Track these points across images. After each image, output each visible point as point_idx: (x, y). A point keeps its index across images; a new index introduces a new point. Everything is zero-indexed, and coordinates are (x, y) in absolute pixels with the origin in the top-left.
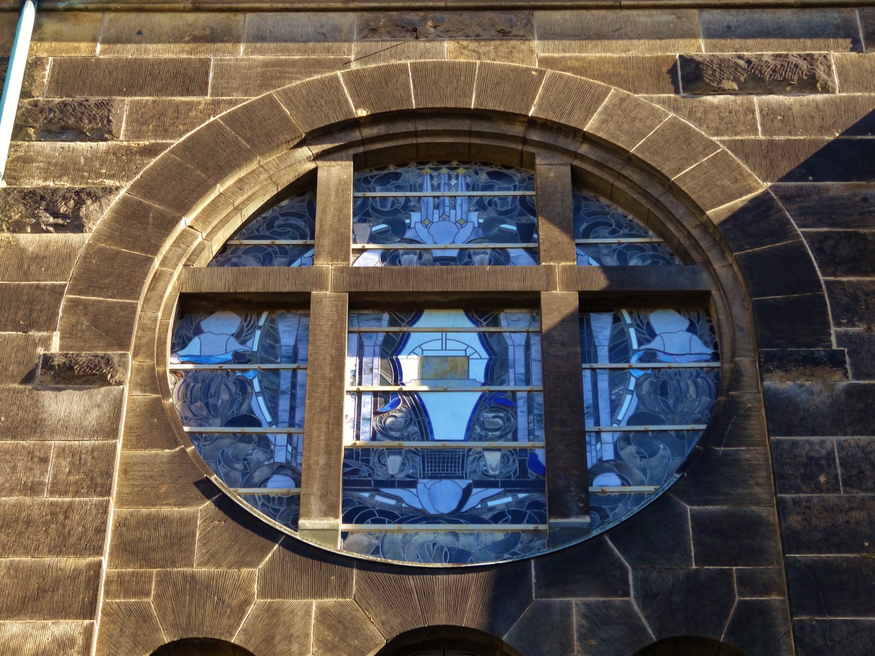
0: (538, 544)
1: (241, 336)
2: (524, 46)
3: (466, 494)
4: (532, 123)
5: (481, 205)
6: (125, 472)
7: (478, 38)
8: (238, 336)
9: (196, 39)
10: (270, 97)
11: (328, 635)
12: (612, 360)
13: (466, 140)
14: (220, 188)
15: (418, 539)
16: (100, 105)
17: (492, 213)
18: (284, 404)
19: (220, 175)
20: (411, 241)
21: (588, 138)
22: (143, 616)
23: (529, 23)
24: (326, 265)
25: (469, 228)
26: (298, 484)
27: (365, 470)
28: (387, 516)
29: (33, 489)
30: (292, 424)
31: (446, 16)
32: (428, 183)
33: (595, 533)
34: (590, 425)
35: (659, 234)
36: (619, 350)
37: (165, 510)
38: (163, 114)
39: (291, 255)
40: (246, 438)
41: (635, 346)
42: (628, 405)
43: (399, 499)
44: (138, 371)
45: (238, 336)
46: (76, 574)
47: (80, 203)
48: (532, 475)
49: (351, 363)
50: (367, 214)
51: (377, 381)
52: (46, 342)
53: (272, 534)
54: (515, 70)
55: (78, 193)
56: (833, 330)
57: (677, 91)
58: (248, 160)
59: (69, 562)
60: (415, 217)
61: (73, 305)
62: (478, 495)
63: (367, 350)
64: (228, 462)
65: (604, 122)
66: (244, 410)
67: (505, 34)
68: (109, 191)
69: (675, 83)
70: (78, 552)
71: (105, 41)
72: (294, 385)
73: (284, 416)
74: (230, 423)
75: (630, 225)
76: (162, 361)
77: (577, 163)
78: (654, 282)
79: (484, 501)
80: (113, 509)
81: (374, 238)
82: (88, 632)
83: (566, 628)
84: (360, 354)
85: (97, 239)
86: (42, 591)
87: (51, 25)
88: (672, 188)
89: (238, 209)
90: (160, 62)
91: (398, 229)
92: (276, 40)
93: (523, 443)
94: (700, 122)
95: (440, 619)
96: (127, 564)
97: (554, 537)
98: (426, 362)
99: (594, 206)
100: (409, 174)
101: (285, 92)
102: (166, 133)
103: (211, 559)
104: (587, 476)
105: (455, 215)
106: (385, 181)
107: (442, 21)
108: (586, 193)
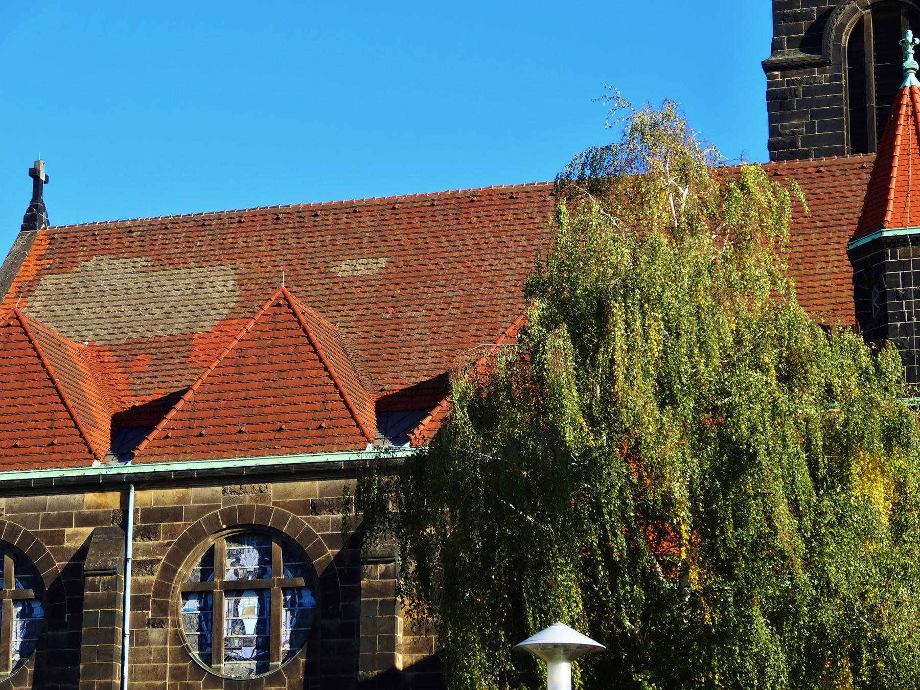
19: (187, 554)
20: (242, 565)
24: (217, 580)
27: (229, 645)
28: (235, 659)
29: (149, 661)
59: (159, 683)
60: (243, 555)
65: (288, 527)
68: (159, 561)
73: (210, 628)
91: (238, 560)
94: (314, 527)
102: (172, 537)
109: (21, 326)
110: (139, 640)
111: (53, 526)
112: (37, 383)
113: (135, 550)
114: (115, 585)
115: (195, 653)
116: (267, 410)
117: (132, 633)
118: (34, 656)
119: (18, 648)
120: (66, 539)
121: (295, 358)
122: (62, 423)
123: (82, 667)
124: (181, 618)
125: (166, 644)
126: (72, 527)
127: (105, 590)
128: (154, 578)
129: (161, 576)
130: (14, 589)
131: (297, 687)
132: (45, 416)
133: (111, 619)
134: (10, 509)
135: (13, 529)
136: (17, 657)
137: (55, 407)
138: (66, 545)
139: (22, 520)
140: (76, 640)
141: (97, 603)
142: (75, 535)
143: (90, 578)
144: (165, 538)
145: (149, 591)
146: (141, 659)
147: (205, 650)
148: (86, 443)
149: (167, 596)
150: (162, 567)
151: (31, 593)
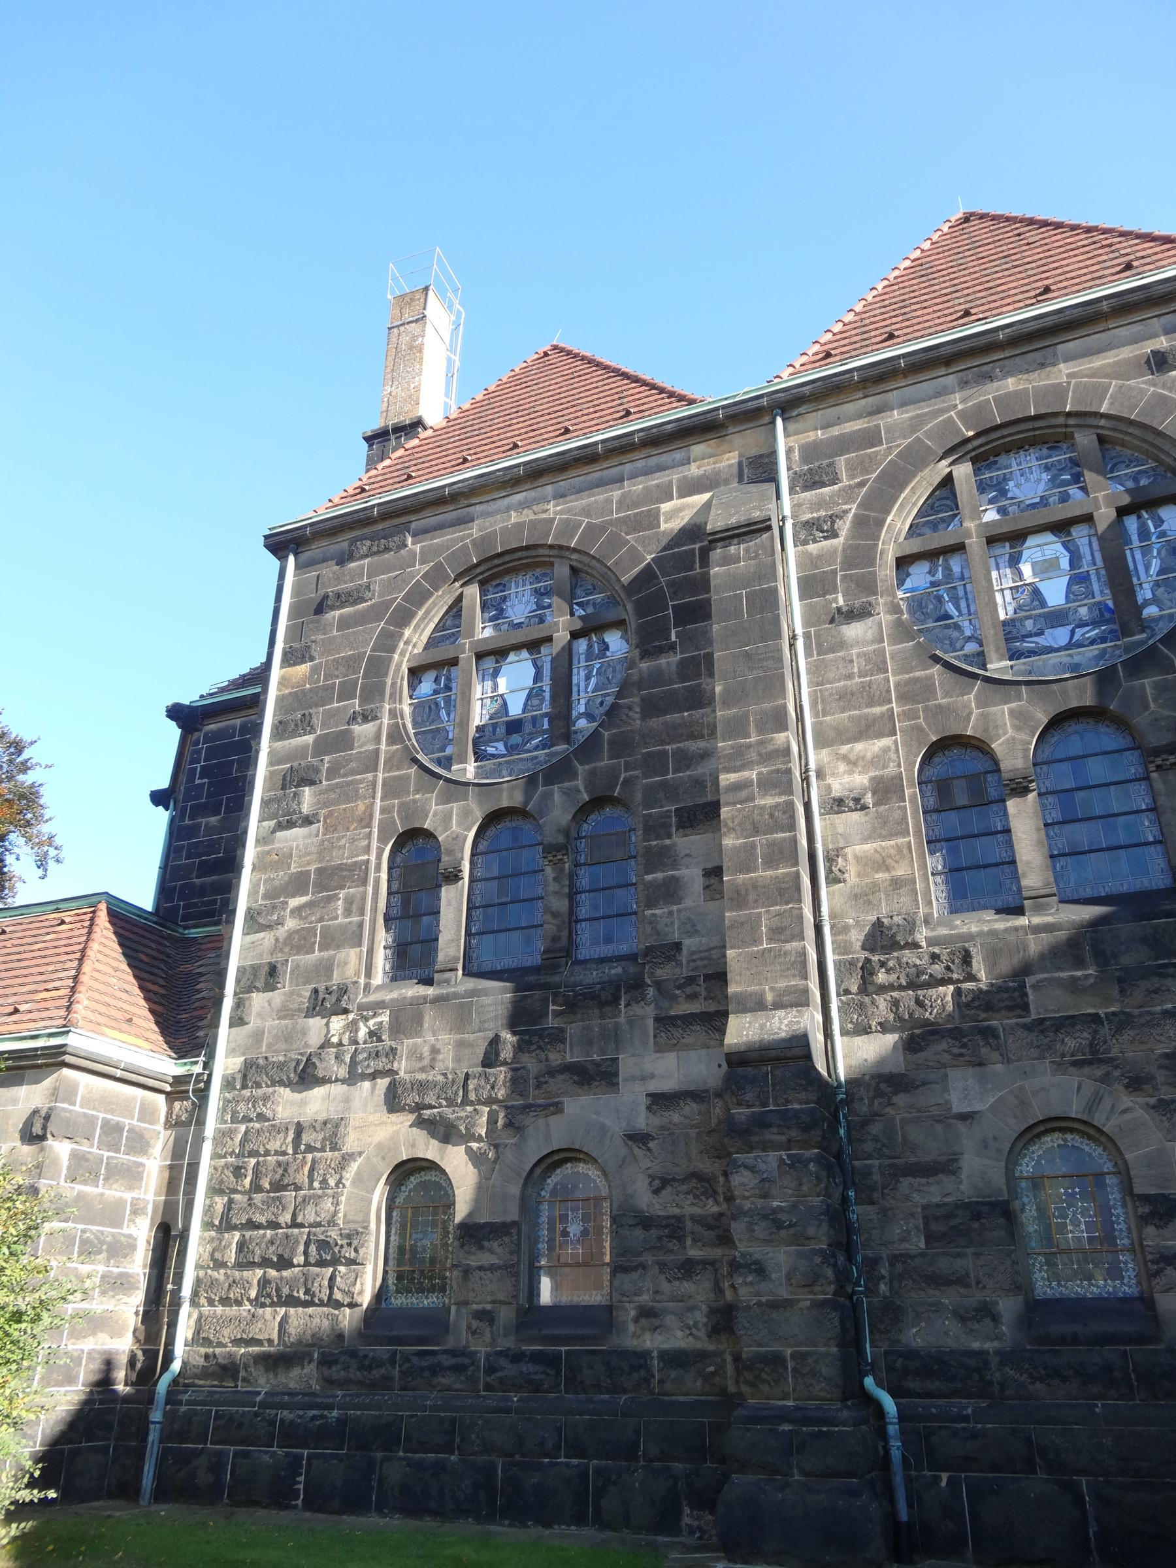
0: (1117, 652)
1: (931, 572)
2: (1055, 369)
3: (1073, 633)
4: (1069, 415)
5: (1047, 468)
6: (892, 658)
7: (1027, 372)
8: (929, 572)
9: (871, 414)
10: (918, 439)
11: (1017, 722)
12: (1141, 541)
13: (1032, 433)
14: (903, 496)
15: (1052, 662)
16: (829, 465)
17: (1054, 471)
18: (963, 604)
19: (902, 488)
21: (1103, 416)
22: (920, 729)
23: (1055, 354)
24: (970, 525)
25: (1043, 482)
26: (981, 645)
28: (1032, 653)
29: (850, 677)
30: (970, 614)
31: (1006, 362)
32: (1014, 463)
33: (1151, 642)
34: (1135, 581)
35: (1156, 461)
36: (1144, 534)
37: (917, 674)
38: (862, 462)
39: (947, 521)
40: (947, 627)
41: (1153, 530)
42: (1155, 565)
43: (1037, 643)
44: (885, 604)
45: (929, 572)
46: (882, 715)
47: (833, 522)
48: (1107, 615)
49: (994, 574)
50: (984, 489)
51: (1010, 581)
52: (836, 600)
53: (975, 676)
54: (1053, 385)
55: (831, 517)
57: (1153, 374)
58: (914, 476)
59: (877, 710)
60: (1011, 484)
61: (844, 578)
62: (1079, 632)
63: (1001, 565)
64: (942, 642)
65: (1112, 404)
66: (942, 612)
67: (1042, 365)
68: (846, 512)
69: (1150, 368)
70: (881, 704)
71: (823, 428)
72: (966, 593)
73: (964, 611)
74: (938, 620)
75: (1137, 460)
76: (895, 596)
77: (1099, 431)
78: (1159, 492)
79: (1083, 635)
81: (991, 502)
82: (896, 742)
83: (1143, 697)
84: (998, 569)
85: (846, 539)
86: (868, 727)
87: (792, 427)
88: (1159, 434)
89: (914, 504)
90: (854, 432)
91: (1003, 493)
92: (914, 403)
93: (1098, 598)
95: (1074, 704)
96: (905, 705)
97: (1127, 649)
98: (1034, 565)
99: (1113, 453)
100: (1002, 460)
101: (925, 432)
102: (868, 472)
103: (947, 694)
104: (1139, 609)
105: (1034, 477)
106: (989, 467)
107: (1004, 366)
108: (1108, 446)
110: (820, 646)
111: (636, 504)
113: (796, 507)
117: (807, 636)
120: (662, 518)
123: (718, 689)
126: (671, 499)
127: (751, 558)
135: (568, 525)
138: (664, 526)
139: (583, 509)
141: (737, 582)
144: (852, 477)
145: (834, 562)
146: (831, 675)
147: (962, 648)
150: (853, 522)
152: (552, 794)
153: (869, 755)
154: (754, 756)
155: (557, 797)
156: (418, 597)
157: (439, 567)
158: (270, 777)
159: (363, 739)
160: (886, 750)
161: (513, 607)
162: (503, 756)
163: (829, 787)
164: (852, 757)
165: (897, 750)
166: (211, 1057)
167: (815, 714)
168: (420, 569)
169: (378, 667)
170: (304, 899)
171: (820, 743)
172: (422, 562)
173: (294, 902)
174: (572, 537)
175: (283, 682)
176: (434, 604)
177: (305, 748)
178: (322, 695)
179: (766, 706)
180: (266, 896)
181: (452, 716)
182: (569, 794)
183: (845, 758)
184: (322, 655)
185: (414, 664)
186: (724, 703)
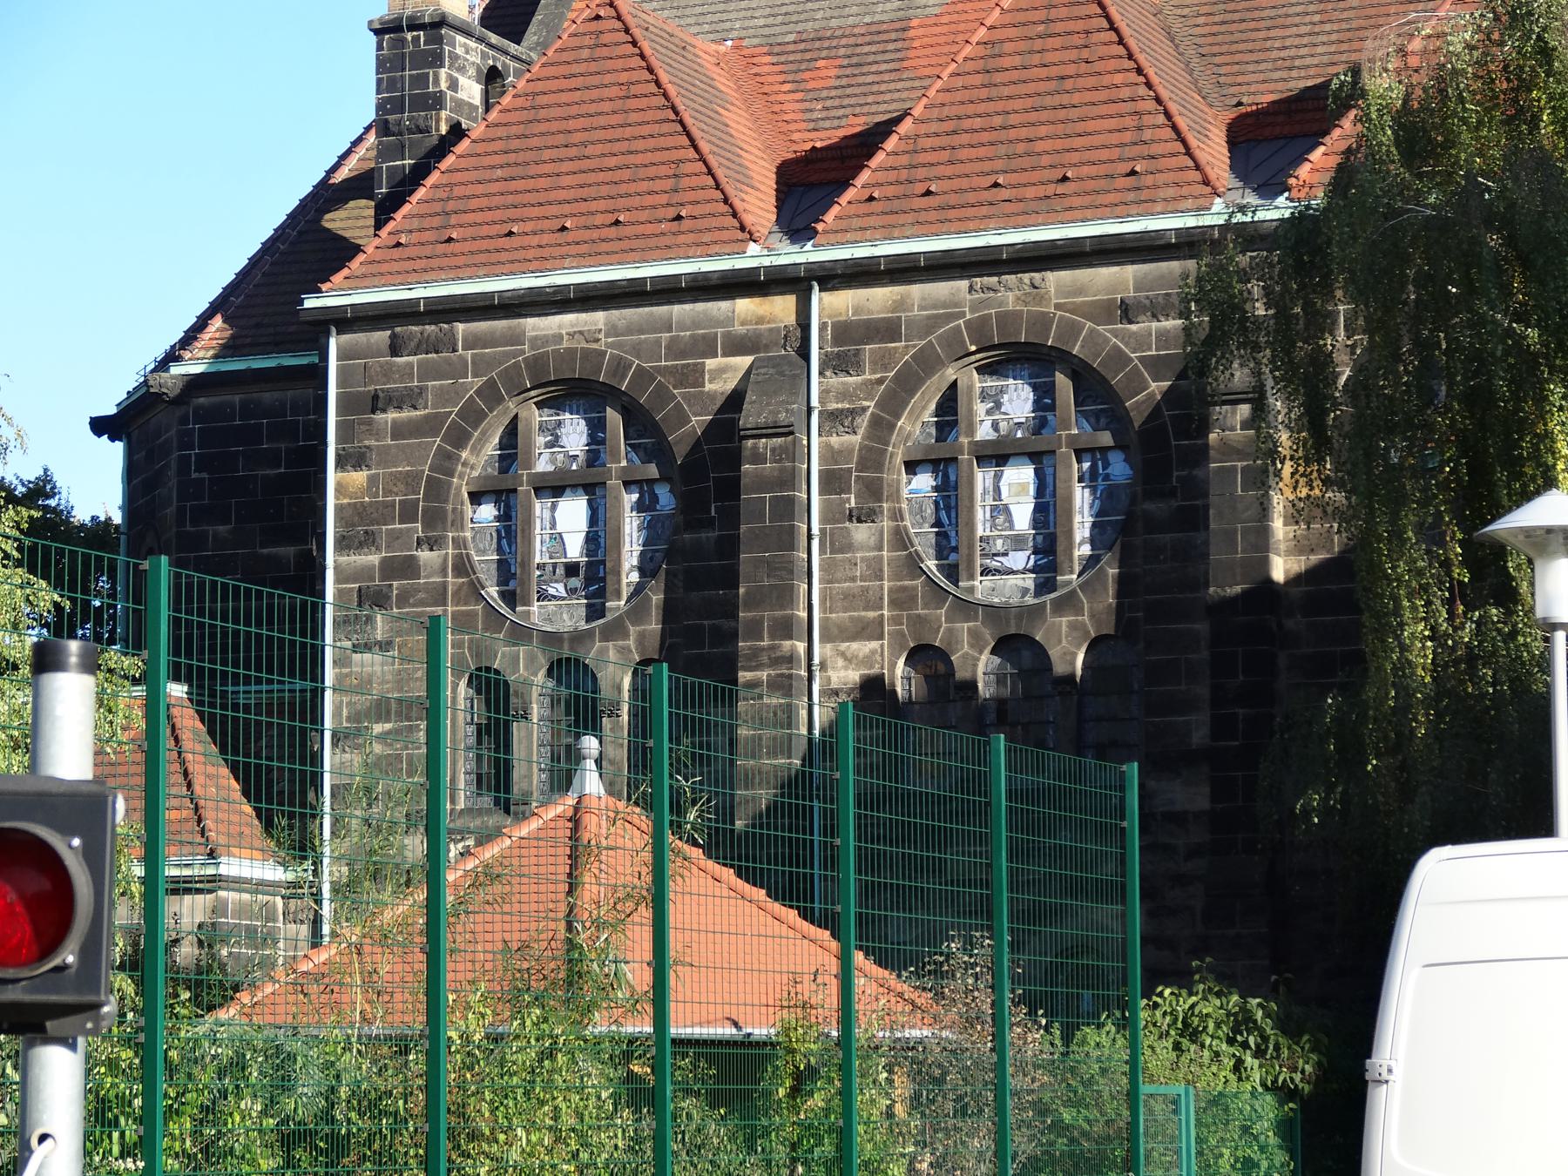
19: (912, 395)
22: (901, 633)
24: (964, 440)
28: (997, 571)
29: (853, 579)
54: (1043, 312)
56: (1175, 474)
59: (872, 614)
60: (1006, 397)
65: (1082, 346)
68: (864, 409)
70: (874, 609)
73: (954, 521)
80: (886, 584)
82: (882, 646)
91: (998, 405)
94: (1126, 345)
95: (1013, 631)
102: (885, 368)
103: (926, 606)
109: (619, 18)
110: (836, 544)
111: (683, 354)
112: (650, 115)
113: (824, 393)
114: (793, 454)
115: (931, 564)
116: (1039, 146)
118: (662, 575)
119: (635, 562)
120: (707, 377)
121: (1085, 54)
122: (694, 181)
123: (742, 591)
124: (904, 506)
125: (880, 549)
128: (856, 439)
129: (867, 437)
130: (624, 463)
131: (1104, 616)
132: (663, 170)
133: (787, 509)
134: (612, 330)
135: (619, 363)
136: (635, 577)
137: (682, 154)
138: (708, 387)
140: (730, 547)
141: (763, 484)
142: (722, 370)
143: (750, 442)
144: (873, 372)
146: (839, 575)
147: (947, 558)
148: (735, 215)
149: (879, 467)
150: (870, 421)
151: (652, 471)
152: (608, 648)
153: (861, 655)
154: (765, 659)
155: (611, 653)
156: (472, 415)
157: (491, 384)
158: (339, 594)
159: (429, 569)
160: (873, 652)
161: (568, 434)
162: (564, 599)
163: (829, 679)
164: (849, 655)
165: (882, 654)
166: (317, 863)
167: (823, 609)
168: (474, 382)
169: (437, 490)
170: (388, 726)
171: (825, 638)
172: (475, 375)
173: (378, 728)
174: (624, 377)
175: (340, 490)
176: (490, 425)
177: (371, 568)
178: (383, 513)
179: (778, 613)
180: (349, 719)
181: (513, 549)
182: (623, 651)
183: (843, 654)
184: (378, 465)
185: (473, 489)
186: (745, 604)
